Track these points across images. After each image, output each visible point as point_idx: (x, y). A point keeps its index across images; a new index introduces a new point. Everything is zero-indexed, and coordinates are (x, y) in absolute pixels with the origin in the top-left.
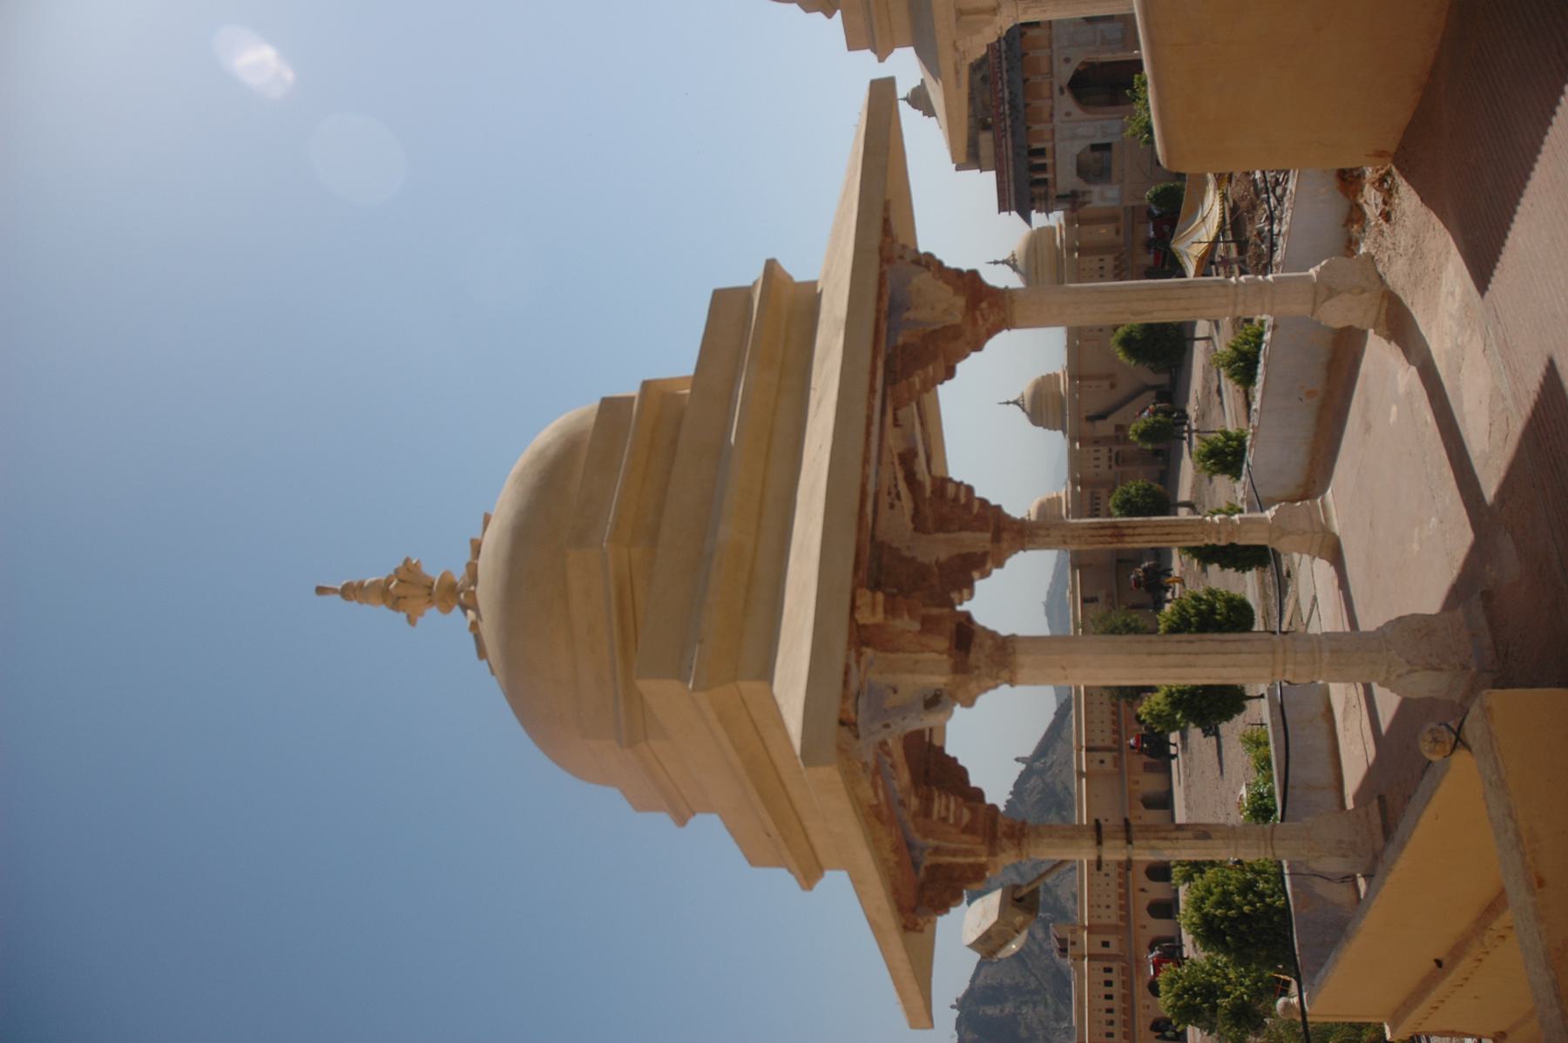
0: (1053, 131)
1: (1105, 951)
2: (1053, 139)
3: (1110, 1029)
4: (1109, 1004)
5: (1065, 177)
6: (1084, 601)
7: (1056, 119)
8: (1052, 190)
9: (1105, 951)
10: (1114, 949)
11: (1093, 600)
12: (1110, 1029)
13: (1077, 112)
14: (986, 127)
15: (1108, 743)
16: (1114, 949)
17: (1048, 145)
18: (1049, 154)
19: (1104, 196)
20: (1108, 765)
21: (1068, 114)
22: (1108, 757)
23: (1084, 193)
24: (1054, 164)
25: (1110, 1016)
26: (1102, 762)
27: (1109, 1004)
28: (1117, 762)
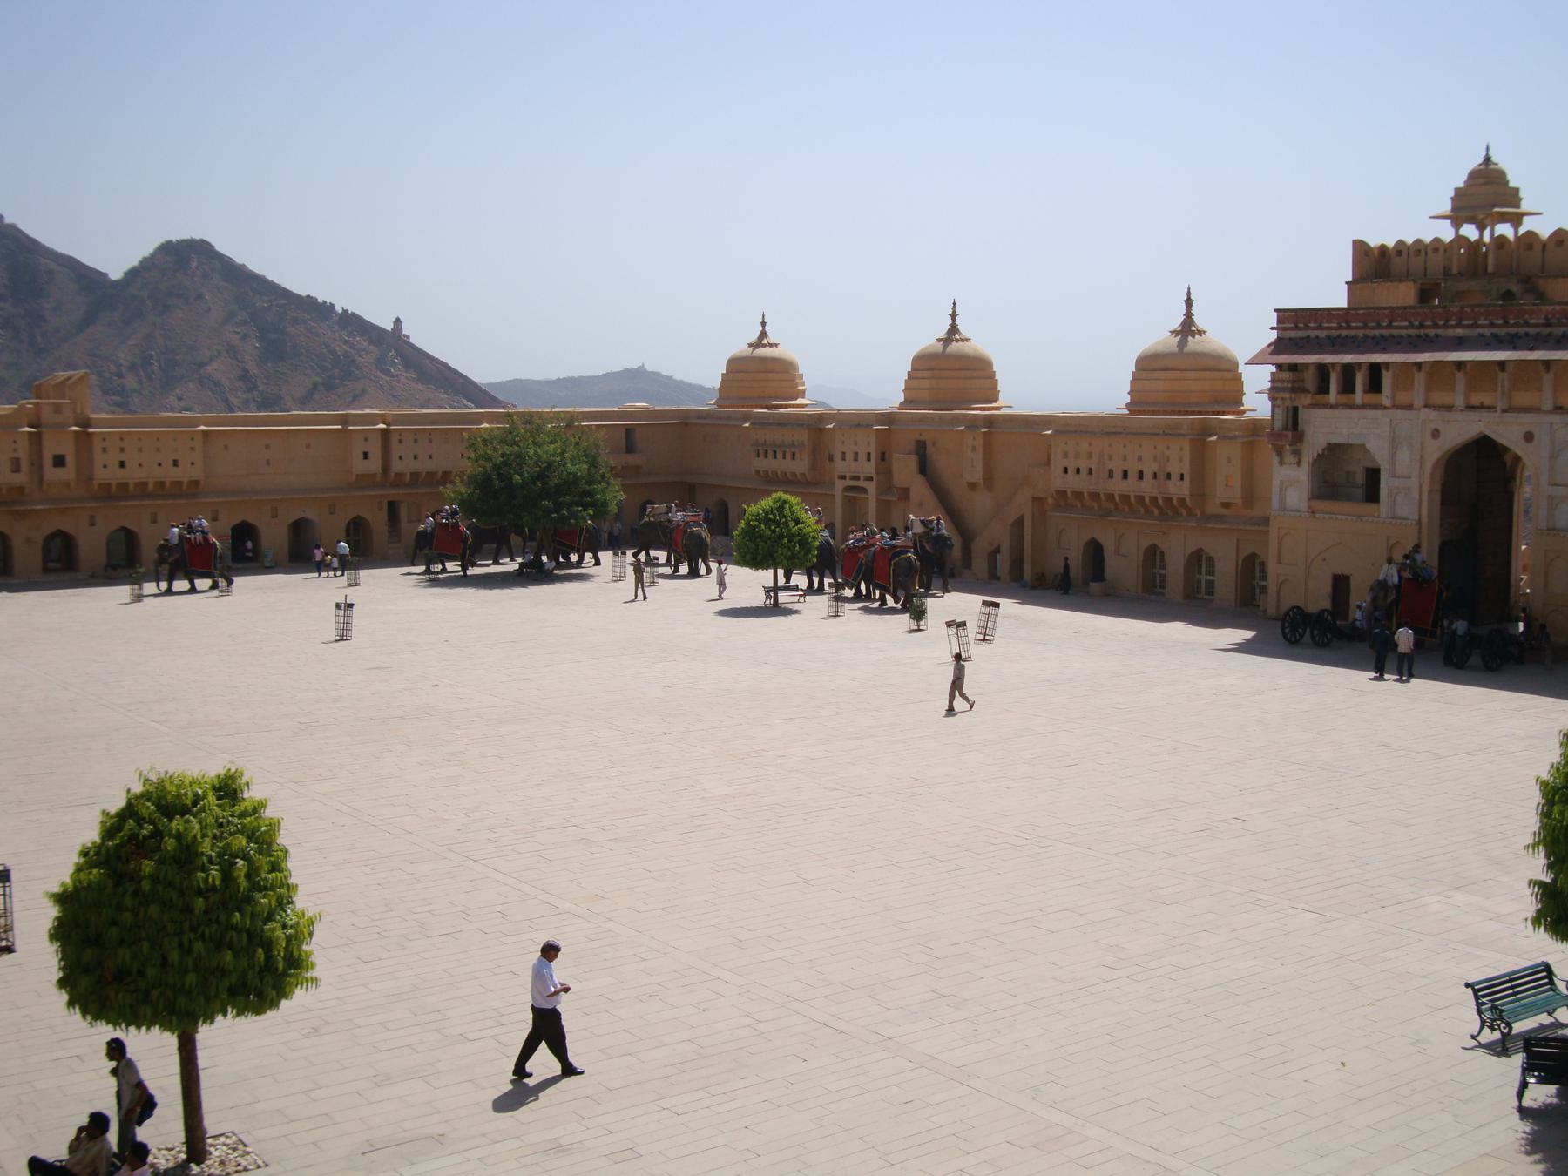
0: (1409, 407)
2: (1396, 406)
5: (1327, 425)
6: (629, 430)
7: (1426, 414)
8: (1307, 399)
11: (630, 448)
13: (1435, 451)
14: (1425, 295)
15: (397, 466)
17: (1385, 397)
18: (1372, 398)
19: (1290, 484)
20: (360, 466)
21: (1436, 434)
22: (374, 465)
23: (1297, 453)
24: (1352, 406)
26: (366, 456)
28: (365, 481)
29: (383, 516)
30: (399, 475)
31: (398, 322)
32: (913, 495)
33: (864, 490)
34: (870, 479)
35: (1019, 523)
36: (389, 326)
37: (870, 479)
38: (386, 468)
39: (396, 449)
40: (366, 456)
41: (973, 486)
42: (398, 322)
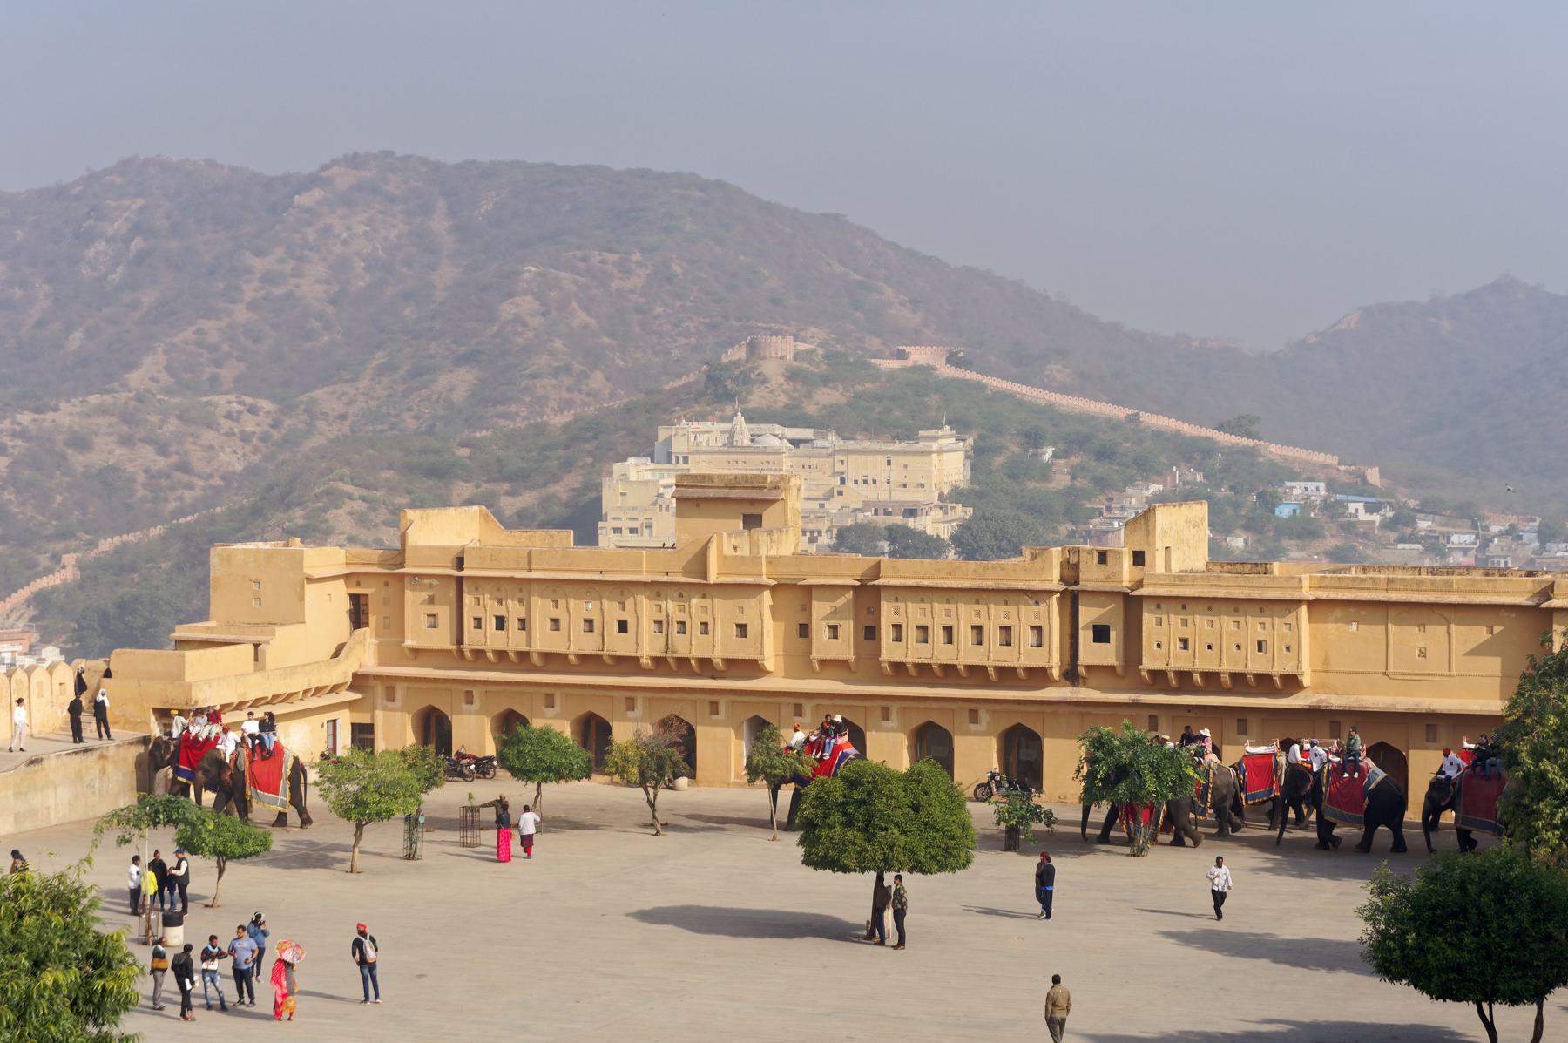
3: (911, 634)
4: (964, 635)
10: (1091, 653)
12: (911, 634)
25: (937, 635)
27: (964, 635)
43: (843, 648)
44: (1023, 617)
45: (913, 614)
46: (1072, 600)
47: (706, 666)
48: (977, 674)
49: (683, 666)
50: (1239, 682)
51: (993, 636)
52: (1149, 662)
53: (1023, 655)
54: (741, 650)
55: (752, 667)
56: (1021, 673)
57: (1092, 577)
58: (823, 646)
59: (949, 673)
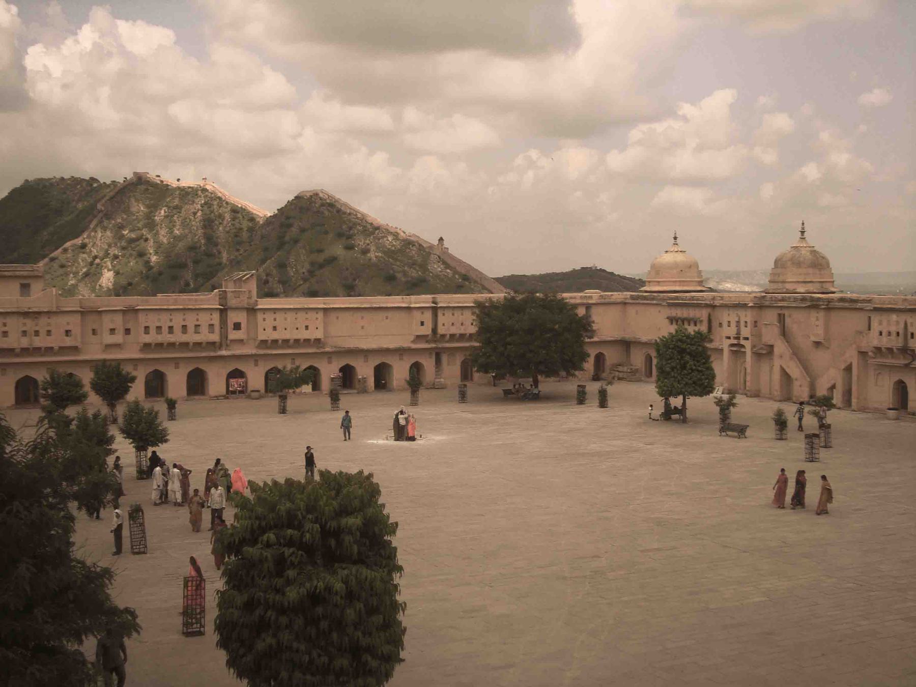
1: (230, 326)
3: (153, 331)
4: (177, 330)
9: (230, 326)
15: (441, 330)
16: (233, 335)
22: (427, 330)
25: (165, 329)
26: (422, 324)
27: (177, 330)
29: (433, 360)
30: (443, 336)
31: (441, 239)
32: (776, 350)
33: (743, 346)
34: (747, 339)
35: (849, 369)
36: (436, 243)
37: (747, 339)
38: (434, 330)
39: (441, 319)
40: (422, 324)
41: (817, 344)
42: (441, 239)
43: (118, 338)
44: (204, 319)
45: (153, 321)
46: (223, 312)
47: (49, 350)
48: (185, 345)
49: (37, 350)
50: (297, 341)
51: (191, 329)
52: (262, 336)
53: (205, 336)
54: (68, 342)
55: (75, 349)
56: (204, 345)
57: (232, 302)
58: (110, 339)
59: (172, 345)
